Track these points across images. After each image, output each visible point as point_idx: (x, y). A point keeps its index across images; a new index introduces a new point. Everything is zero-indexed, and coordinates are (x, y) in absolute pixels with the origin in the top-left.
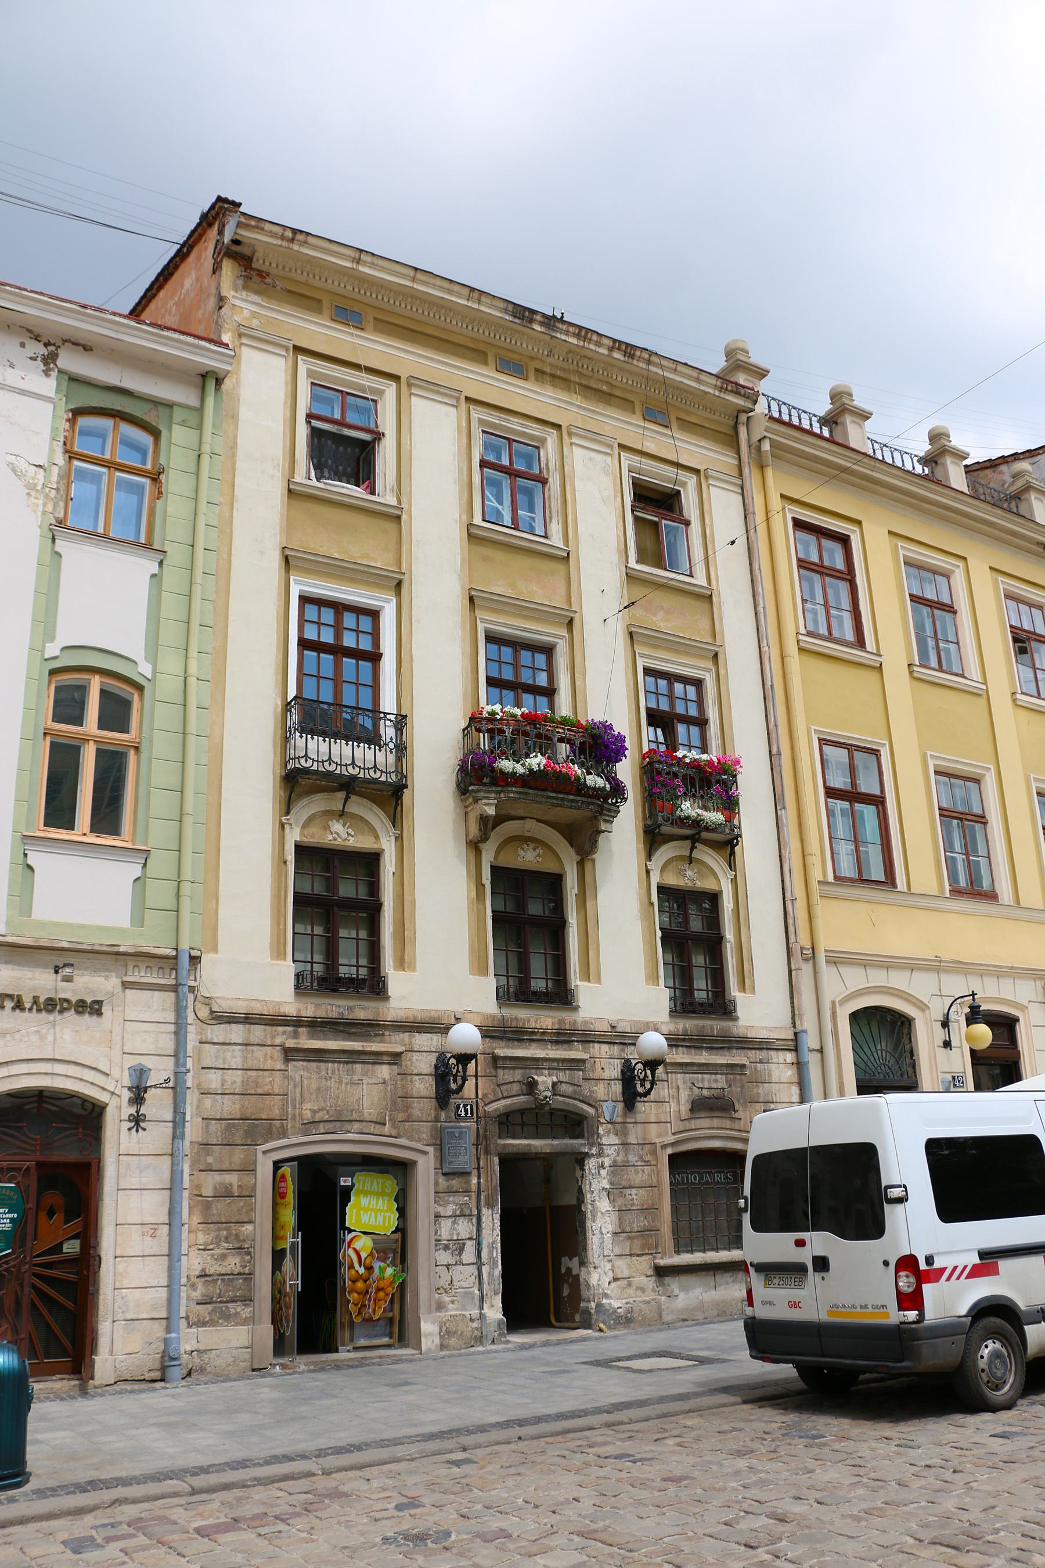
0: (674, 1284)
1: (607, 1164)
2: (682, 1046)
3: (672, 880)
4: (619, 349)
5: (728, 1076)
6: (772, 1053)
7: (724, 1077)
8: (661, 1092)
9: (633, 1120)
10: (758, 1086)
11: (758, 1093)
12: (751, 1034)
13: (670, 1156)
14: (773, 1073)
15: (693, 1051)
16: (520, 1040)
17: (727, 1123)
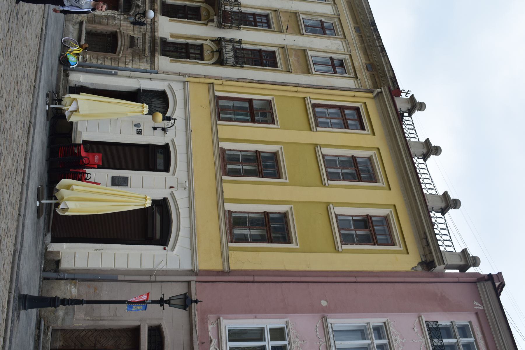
0: (77, 26)
1: (115, 15)
2: (151, 39)
3: (205, 47)
4: (381, 47)
5: (142, 50)
6: (150, 65)
7: (141, 48)
8: (136, 32)
9: (128, 23)
10: (138, 58)
11: (136, 58)
12: (156, 58)
13: (116, 31)
14: (142, 64)
15: (150, 42)
16: (151, 2)
17: (126, 47)
